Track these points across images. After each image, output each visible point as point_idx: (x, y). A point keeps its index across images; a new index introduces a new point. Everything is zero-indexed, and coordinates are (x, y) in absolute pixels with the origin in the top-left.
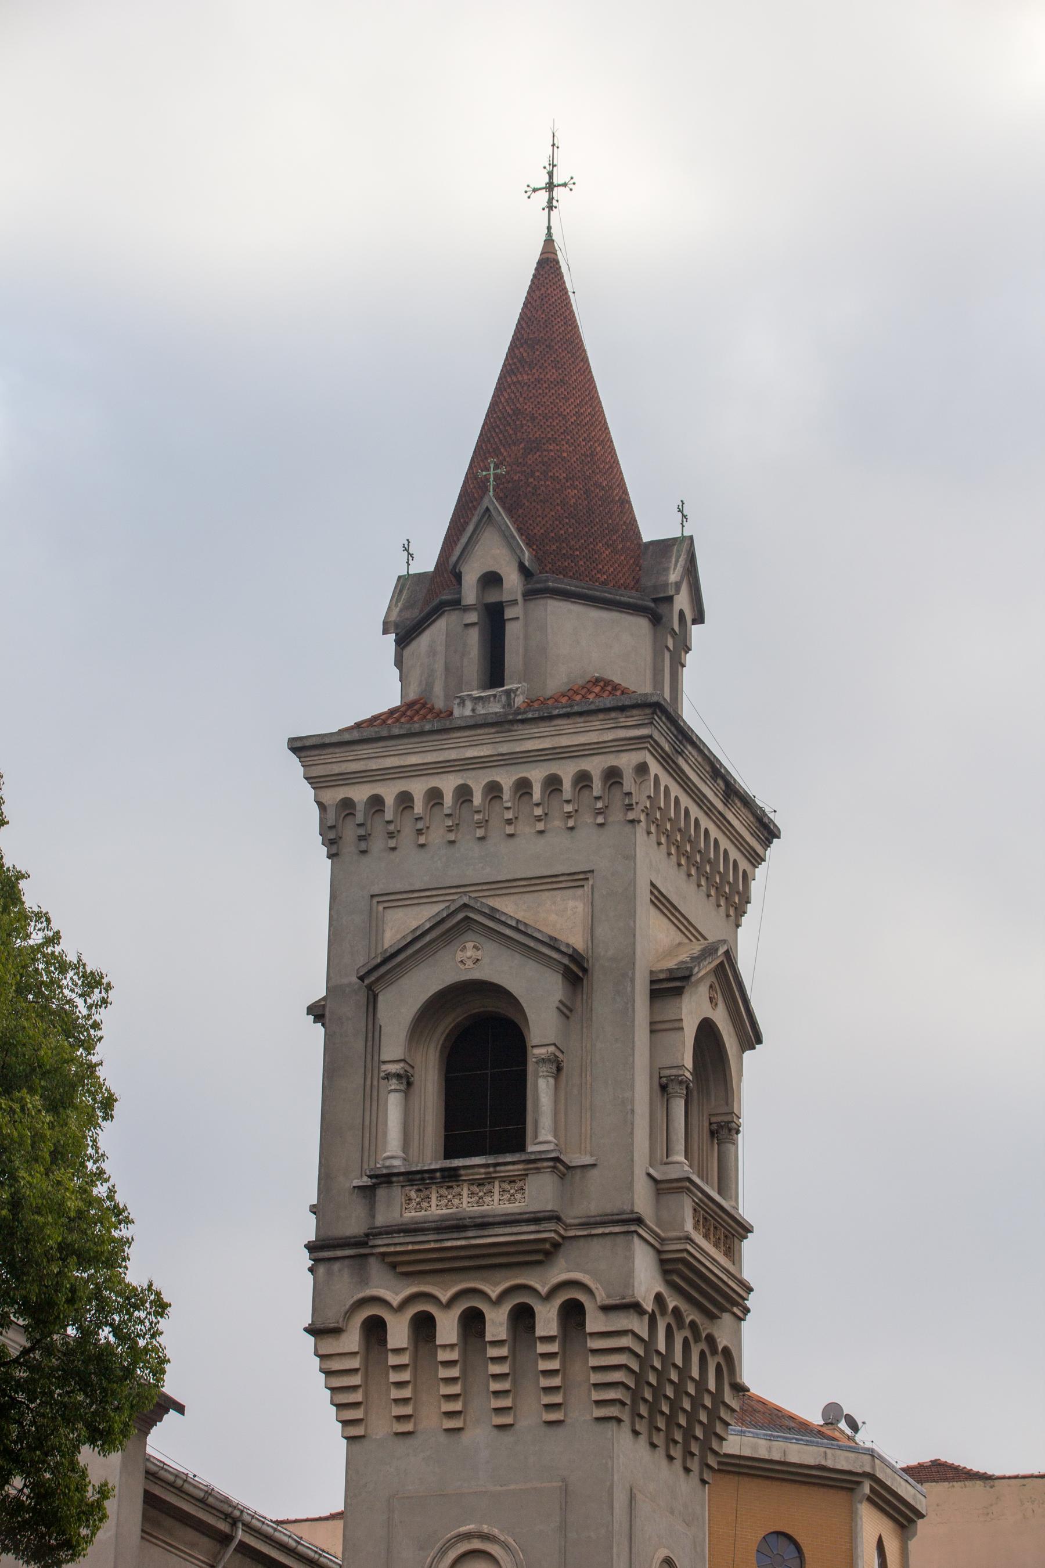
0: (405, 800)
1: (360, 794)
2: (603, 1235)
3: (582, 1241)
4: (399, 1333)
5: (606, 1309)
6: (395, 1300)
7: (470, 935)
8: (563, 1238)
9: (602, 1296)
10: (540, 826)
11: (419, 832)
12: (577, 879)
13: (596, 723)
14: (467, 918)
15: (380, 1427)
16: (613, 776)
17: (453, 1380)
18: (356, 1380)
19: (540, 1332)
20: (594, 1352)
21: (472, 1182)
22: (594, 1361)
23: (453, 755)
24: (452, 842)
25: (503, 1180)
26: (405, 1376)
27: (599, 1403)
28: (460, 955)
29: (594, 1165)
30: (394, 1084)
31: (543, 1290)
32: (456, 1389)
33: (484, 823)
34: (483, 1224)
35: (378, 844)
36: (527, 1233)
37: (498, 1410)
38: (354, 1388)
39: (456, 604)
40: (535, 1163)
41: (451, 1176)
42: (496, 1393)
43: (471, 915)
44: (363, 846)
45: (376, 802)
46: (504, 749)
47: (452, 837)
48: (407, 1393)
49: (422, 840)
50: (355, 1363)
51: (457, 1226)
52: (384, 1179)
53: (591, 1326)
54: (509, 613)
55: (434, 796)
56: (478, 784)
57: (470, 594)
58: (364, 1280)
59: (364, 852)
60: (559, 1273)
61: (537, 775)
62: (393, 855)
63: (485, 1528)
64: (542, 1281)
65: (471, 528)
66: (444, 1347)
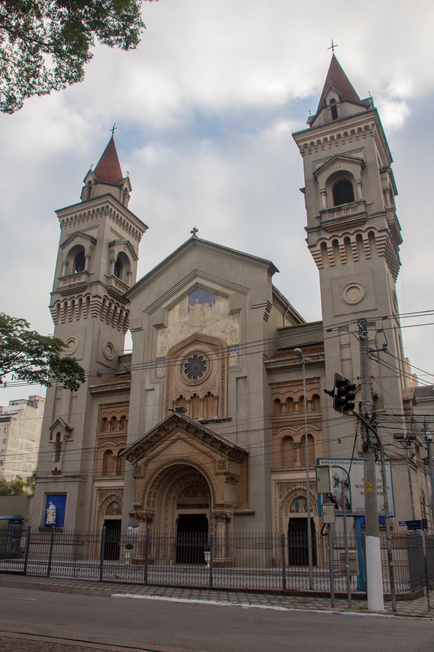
0: (319, 142)
1: (308, 142)
2: (377, 217)
3: (372, 219)
4: (329, 244)
5: (380, 231)
6: (328, 237)
7: (337, 162)
8: (368, 219)
9: (378, 229)
10: (350, 141)
11: (323, 147)
12: (360, 150)
13: (362, 117)
14: (337, 158)
15: (326, 265)
16: (367, 128)
17: (344, 252)
18: (320, 256)
19: (364, 239)
20: (378, 241)
21: (344, 210)
22: (377, 243)
23: (329, 130)
24: (330, 148)
25: (352, 208)
26: (332, 253)
27: (379, 253)
28: (336, 167)
29: (372, 203)
30: (323, 194)
31: (364, 230)
32: (344, 254)
33: (337, 143)
34: (348, 217)
35: (313, 152)
36: (359, 217)
37: (354, 258)
38: (320, 258)
39: (326, 107)
40: (359, 203)
41: (339, 209)
42: (354, 254)
43: (338, 157)
44: (310, 152)
45: (312, 143)
46: (341, 126)
47: (330, 147)
48: (332, 257)
49: (323, 149)
50: (320, 252)
51: (342, 218)
52: (323, 212)
53: (376, 236)
54: (337, 105)
55: (325, 139)
56: (335, 135)
57: (328, 103)
58: (320, 235)
59: (310, 154)
60: (367, 226)
61: (349, 131)
62: (317, 153)
63: (355, 282)
64: (363, 228)
65: (327, 91)
66: (341, 246)
